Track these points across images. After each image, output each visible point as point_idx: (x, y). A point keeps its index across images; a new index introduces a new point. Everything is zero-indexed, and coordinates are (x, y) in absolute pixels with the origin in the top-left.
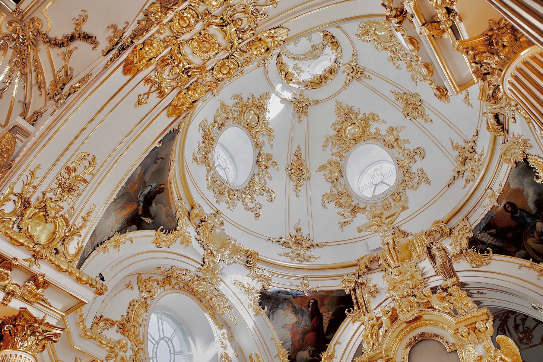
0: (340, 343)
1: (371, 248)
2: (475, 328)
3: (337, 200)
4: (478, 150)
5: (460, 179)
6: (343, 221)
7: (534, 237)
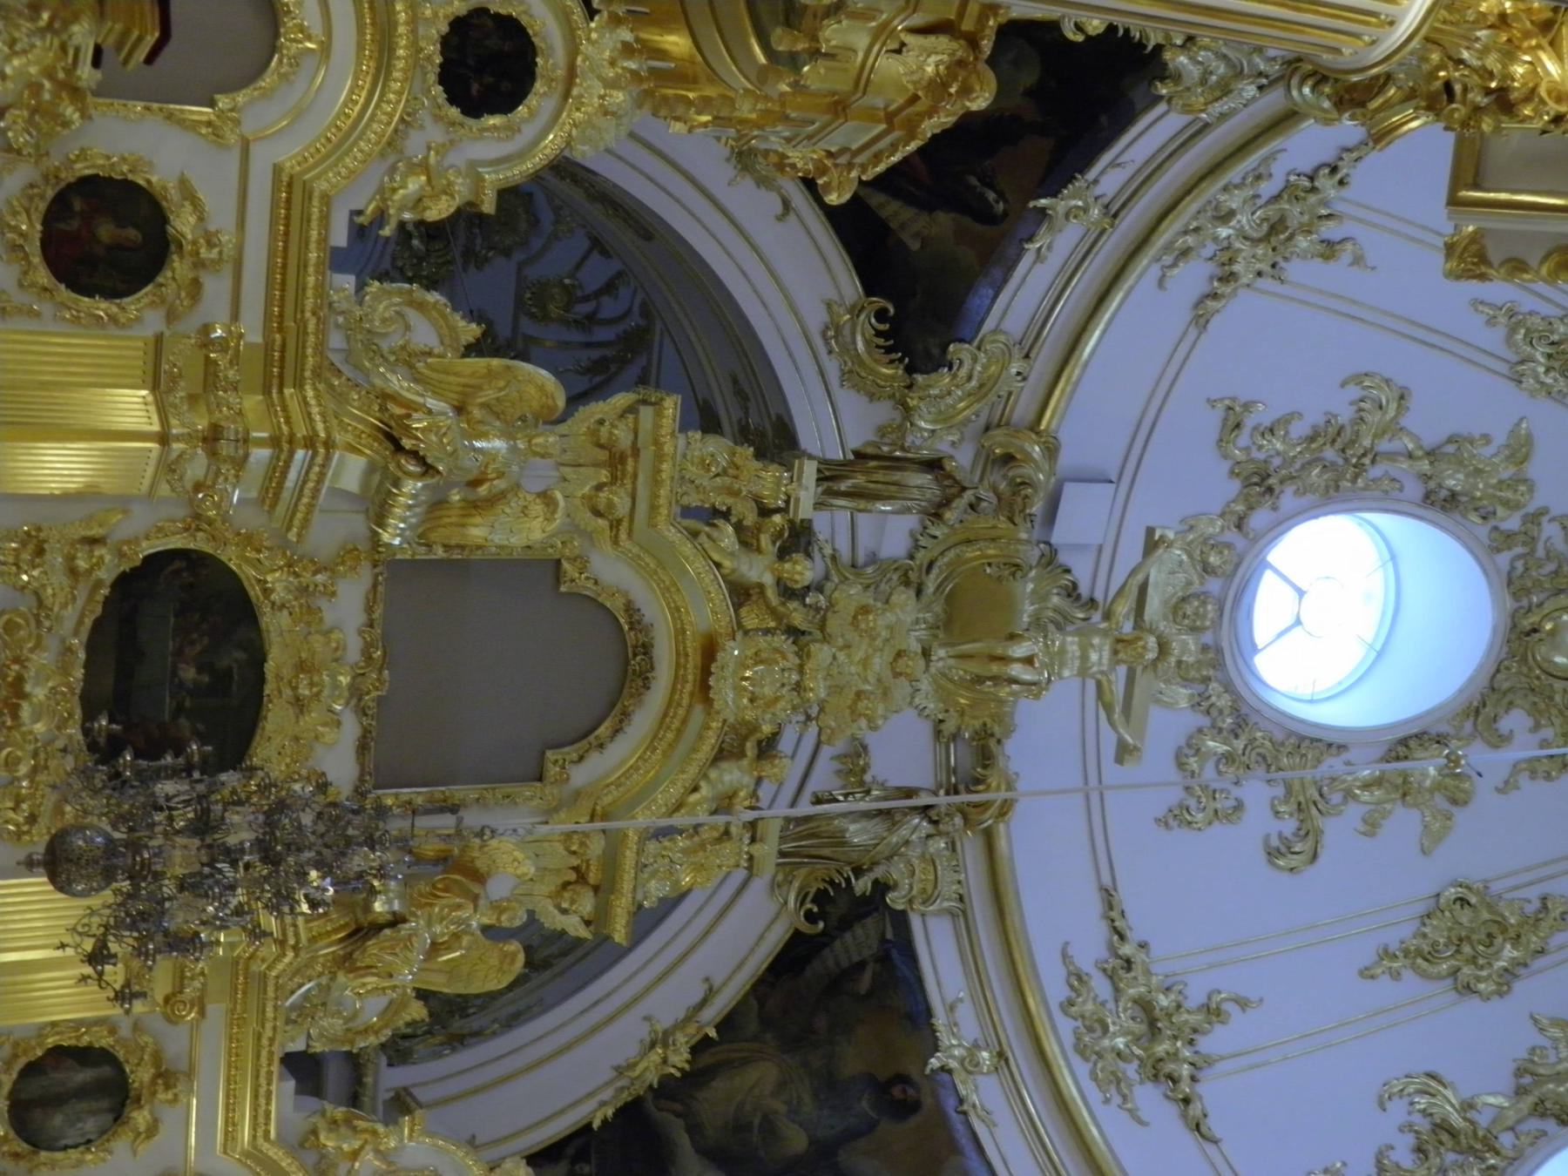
0: (781, 218)
1: (1070, 490)
3: (1348, 434)
4: (1148, 1096)
5: (1104, 953)
6: (1249, 422)
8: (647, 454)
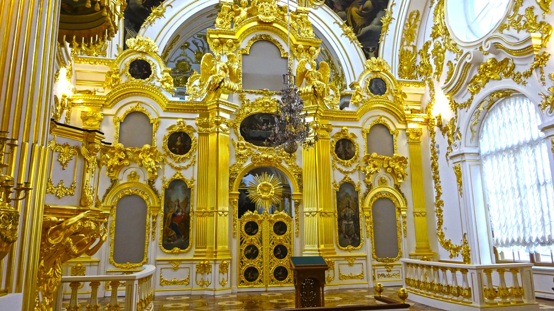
0: (172, 7)
2: (308, 49)
7: (359, 8)
8: (220, 36)
